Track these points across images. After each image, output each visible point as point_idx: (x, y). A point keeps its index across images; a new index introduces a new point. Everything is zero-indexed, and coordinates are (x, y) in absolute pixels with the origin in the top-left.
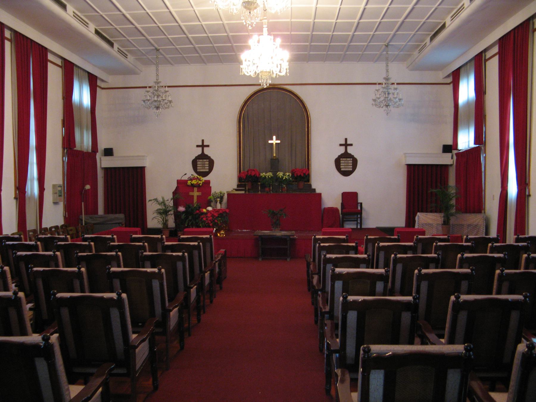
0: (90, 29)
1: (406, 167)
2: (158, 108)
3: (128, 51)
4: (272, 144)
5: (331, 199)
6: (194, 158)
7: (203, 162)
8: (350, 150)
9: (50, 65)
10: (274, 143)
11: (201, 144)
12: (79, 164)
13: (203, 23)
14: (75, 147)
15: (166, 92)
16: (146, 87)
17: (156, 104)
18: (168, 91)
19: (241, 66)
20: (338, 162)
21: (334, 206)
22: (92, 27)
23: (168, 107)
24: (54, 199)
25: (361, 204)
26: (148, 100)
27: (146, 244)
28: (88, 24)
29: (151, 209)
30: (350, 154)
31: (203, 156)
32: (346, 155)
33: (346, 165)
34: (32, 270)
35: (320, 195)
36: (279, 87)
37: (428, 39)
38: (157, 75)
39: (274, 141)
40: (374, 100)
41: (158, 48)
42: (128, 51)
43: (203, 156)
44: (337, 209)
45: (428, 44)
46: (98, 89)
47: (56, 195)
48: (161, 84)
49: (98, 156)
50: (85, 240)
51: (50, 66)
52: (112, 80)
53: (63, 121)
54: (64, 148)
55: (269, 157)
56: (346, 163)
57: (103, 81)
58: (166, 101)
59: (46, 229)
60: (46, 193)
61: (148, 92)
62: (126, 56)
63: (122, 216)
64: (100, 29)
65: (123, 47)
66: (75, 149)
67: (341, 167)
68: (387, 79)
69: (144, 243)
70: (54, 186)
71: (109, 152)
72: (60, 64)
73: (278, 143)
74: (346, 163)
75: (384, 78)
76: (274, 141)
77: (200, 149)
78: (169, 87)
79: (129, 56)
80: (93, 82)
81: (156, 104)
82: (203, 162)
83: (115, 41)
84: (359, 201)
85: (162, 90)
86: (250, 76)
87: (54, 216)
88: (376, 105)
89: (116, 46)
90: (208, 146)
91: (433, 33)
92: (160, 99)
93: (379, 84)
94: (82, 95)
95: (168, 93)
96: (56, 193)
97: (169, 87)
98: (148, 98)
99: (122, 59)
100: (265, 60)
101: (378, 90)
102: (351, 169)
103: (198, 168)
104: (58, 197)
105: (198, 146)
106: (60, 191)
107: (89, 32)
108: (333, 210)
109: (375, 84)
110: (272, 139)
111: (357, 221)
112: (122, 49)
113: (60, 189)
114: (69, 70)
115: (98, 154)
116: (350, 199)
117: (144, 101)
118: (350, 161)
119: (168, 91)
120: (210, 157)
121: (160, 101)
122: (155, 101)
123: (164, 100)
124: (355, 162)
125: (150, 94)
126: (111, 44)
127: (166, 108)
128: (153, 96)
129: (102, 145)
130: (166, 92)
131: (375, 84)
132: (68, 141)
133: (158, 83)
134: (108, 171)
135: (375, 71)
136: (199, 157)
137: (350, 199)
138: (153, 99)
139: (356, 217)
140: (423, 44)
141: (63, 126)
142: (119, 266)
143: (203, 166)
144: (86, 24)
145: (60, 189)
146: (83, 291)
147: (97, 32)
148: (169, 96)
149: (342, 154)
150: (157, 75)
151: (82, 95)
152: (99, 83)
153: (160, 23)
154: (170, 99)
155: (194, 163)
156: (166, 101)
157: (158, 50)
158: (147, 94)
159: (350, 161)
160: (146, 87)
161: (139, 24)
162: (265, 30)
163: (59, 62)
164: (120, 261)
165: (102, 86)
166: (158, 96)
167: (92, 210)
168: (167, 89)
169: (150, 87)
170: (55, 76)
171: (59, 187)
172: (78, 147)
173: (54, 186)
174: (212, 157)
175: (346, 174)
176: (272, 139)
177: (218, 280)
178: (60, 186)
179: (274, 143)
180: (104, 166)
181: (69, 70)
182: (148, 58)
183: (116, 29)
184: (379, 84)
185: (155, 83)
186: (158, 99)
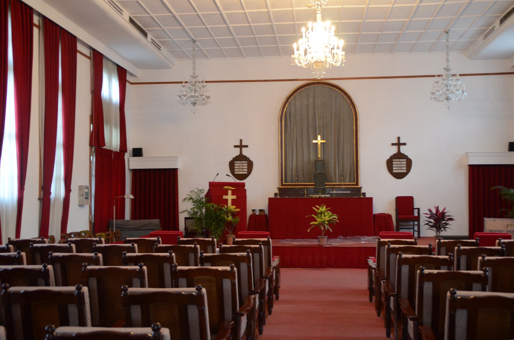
0: (124, 17)
1: (468, 167)
2: (194, 104)
3: (162, 42)
4: (317, 144)
5: (383, 204)
6: (231, 159)
7: (241, 164)
8: (404, 150)
9: (78, 55)
10: (319, 143)
11: (239, 144)
12: (109, 165)
13: (247, 11)
14: (105, 145)
15: (204, 86)
16: (182, 82)
17: (192, 99)
18: (206, 86)
19: (293, 56)
20: (390, 163)
21: (386, 212)
22: (126, 15)
23: (205, 104)
24: (79, 202)
25: (419, 209)
26: (185, 96)
27: (198, 246)
28: (122, 11)
29: (182, 217)
30: (403, 155)
31: (241, 158)
32: (399, 155)
33: (399, 166)
34: (85, 269)
35: (371, 199)
36: (324, 81)
37: (498, 21)
38: (194, 68)
39: (319, 140)
40: (433, 93)
41: (195, 39)
42: (162, 42)
43: (241, 158)
44: (389, 216)
45: (496, 28)
46: (127, 84)
47: (82, 197)
48: (200, 79)
49: (127, 156)
50: (129, 242)
51: (79, 56)
52: (141, 75)
53: (92, 117)
54: (91, 145)
55: (313, 158)
56: (399, 164)
57: (132, 75)
58: (204, 97)
59: (70, 235)
60: (72, 195)
61: (184, 86)
62: (159, 48)
63: (157, 221)
64: (134, 17)
65: (157, 38)
66: (104, 147)
67: (394, 168)
68: (447, 70)
69: (195, 245)
70: (81, 188)
71: (138, 152)
72: (89, 55)
73: (323, 143)
74: (399, 164)
75: (445, 69)
76: (319, 140)
77: (238, 149)
78: (206, 82)
79: (163, 48)
80: (122, 74)
81: (192, 99)
82: (241, 164)
83: (148, 30)
84: (415, 207)
85: (200, 85)
86: (301, 67)
87: (80, 220)
88: (435, 98)
89: (149, 36)
90: (247, 146)
91: (504, 14)
92: (197, 94)
93: (439, 76)
94: (110, 89)
95: (206, 88)
96: (83, 195)
97: (206, 82)
98: (185, 93)
99: (156, 50)
100: (319, 48)
101: (437, 82)
102: (405, 171)
103: (236, 170)
104: (85, 200)
105: (235, 146)
106: (87, 193)
107: (123, 20)
108: (386, 217)
109: (434, 76)
110: (316, 139)
111: (413, 228)
112: (155, 40)
113: (86, 190)
114: (98, 60)
115: (126, 154)
116: (405, 204)
117: (180, 97)
118: (404, 162)
119: (206, 86)
120: (248, 158)
121: (197, 97)
122: (192, 96)
123: (201, 95)
124: (409, 163)
125: (186, 88)
126: (145, 34)
127: (203, 104)
128: (189, 91)
129: (131, 145)
130: (204, 86)
131: (434, 76)
132: (97, 139)
133: (195, 77)
134: (135, 172)
135: (434, 62)
136: (236, 159)
137: (405, 204)
138: (189, 95)
139: (412, 223)
140: (491, 28)
141: (92, 122)
142: (143, 285)
143: (241, 168)
144: (120, 11)
145: (86, 190)
146: (196, 265)
147: (131, 21)
148: (206, 91)
149: (394, 155)
150: (194, 68)
151: (110, 89)
152: (129, 78)
153: (200, 11)
154: (208, 95)
155: (232, 165)
156: (204, 97)
157: (194, 41)
158: (183, 89)
159: (404, 162)
160: (182, 82)
161: (177, 12)
162: (319, 16)
163: (87, 52)
164: (144, 278)
165: (131, 81)
166: (195, 91)
167: (121, 215)
168: (204, 84)
169: (186, 82)
170: (84, 67)
171: (86, 188)
172: (107, 147)
173: (81, 188)
174: (251, 159)
175: (399, 176)
176: (316, 139)
177: (275, 290)
178: (87, 188)
179: (319, 143)
180: (132, 167)
181: (98, 60)
182: (183, 51)
183: (151, 17)
184: (439, 76)
185: (192, 77)
186: (195, 93)
